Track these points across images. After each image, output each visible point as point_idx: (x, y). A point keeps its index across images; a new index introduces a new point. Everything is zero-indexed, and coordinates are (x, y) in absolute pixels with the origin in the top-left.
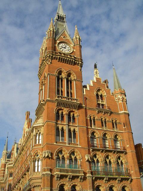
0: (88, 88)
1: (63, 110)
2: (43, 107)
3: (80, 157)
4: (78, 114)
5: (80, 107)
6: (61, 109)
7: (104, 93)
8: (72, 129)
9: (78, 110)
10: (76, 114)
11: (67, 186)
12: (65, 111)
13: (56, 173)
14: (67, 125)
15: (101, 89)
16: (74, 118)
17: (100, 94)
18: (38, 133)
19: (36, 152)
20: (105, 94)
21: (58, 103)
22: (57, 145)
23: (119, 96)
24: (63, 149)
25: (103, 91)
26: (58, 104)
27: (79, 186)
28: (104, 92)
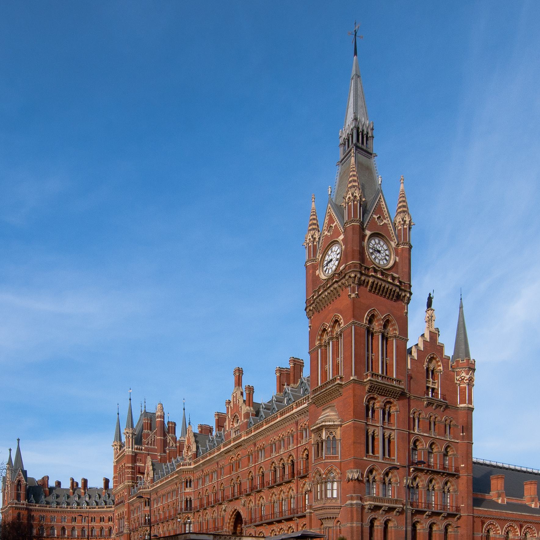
0: (415, 354)
1: (375, 399)
2: (340, 390)
3: (396, 481)
4: (397, 407)
5: (402, 395)
6: (373, 398)
7: (440, 366)
8: (387, 435)
9: (399, 399)
10: (394, 408)
11: (380, 520)
12: (378, 402)
13: (367, 503)
14: (381, 426)
15: (435, 356)
16: (389, 415)
17: (431, 367)
18: (331, 436)
19: (330, 468)
20: (441, 368)
21: (371, 387)
22: (369, 460)
23: (464, 374)
24: (376, 467)
25: (437, 362)
26: (370, 389)
27: (394, 521)
28: (439, 363)
